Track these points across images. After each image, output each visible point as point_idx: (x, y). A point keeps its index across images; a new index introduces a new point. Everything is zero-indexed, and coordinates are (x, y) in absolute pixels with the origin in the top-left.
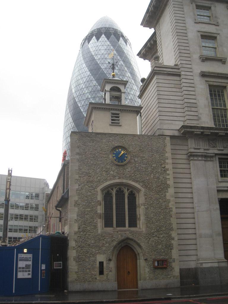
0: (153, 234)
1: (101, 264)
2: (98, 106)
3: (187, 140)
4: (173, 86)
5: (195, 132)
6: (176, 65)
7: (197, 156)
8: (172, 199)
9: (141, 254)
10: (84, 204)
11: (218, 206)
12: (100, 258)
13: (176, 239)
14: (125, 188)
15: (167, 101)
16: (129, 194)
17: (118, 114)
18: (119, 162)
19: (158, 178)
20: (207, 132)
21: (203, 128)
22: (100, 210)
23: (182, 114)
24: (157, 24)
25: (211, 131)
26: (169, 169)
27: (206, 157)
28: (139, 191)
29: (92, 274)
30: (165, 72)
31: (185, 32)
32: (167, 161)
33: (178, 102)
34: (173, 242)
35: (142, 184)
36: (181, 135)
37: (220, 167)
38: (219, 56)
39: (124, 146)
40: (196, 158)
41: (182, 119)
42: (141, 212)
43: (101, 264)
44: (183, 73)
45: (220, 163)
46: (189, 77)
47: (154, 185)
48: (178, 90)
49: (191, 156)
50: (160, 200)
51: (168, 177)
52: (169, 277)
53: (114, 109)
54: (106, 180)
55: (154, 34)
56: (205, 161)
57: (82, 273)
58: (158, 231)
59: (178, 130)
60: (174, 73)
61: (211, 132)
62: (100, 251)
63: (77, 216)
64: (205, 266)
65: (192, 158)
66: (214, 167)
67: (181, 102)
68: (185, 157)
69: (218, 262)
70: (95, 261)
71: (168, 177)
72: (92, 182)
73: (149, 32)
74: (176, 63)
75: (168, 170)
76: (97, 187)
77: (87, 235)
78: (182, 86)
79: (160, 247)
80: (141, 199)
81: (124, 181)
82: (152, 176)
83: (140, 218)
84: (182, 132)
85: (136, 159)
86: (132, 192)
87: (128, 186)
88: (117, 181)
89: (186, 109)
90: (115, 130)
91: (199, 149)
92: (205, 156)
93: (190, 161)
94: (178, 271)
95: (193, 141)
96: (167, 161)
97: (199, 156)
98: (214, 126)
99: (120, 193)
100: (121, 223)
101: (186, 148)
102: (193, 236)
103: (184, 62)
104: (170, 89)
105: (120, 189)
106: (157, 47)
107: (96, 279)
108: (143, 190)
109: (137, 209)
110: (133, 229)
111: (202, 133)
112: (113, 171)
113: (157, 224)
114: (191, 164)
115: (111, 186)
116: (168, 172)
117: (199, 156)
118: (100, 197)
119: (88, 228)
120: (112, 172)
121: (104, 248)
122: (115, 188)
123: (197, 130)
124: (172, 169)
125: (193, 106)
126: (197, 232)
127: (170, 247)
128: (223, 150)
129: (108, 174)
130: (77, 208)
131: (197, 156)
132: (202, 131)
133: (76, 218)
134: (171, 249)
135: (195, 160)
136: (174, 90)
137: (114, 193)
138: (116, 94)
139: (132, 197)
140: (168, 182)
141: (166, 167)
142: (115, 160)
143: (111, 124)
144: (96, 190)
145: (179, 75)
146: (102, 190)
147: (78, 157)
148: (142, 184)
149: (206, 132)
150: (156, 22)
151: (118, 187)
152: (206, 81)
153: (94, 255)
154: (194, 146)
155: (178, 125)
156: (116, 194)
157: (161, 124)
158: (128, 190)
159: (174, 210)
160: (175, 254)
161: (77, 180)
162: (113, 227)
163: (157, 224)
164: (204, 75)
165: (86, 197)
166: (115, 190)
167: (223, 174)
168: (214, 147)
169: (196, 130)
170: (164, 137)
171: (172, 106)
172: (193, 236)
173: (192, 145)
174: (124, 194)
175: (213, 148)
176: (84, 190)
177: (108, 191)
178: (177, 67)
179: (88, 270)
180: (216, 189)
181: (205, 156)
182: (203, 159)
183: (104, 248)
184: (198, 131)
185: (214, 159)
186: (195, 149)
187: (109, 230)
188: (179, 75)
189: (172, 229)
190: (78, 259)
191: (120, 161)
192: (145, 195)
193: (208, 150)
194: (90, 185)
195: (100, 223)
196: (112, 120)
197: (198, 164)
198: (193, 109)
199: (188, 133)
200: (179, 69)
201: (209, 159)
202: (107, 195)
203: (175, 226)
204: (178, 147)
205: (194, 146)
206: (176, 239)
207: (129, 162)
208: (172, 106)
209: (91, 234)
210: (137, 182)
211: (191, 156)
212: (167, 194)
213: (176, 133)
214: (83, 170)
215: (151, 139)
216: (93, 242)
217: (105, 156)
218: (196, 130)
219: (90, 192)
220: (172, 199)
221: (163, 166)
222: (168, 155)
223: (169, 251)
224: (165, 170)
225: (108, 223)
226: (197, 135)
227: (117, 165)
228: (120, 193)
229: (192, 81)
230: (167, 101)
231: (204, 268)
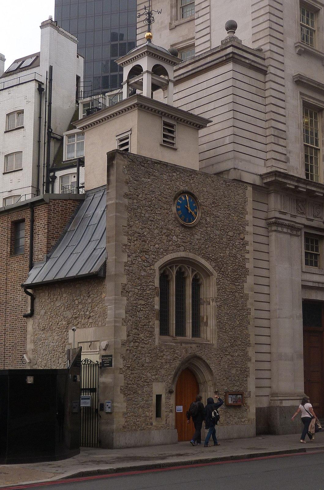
0: (226, 351)
1: (159, 397)
3: (268, 193)
4: (254, 90)
5: (288, 186)
6: (259, 50)
8: (251, 294)
9: (210, 383)
10: (136, 291)
11: (299, 312)
12: (159, 388)
14: (189, 268)
17: (172, 126)
18: (185, 220)
19: (235, 257)
20: (291, 184)
25: (308, 187)
26: (249, 243)
27: (293, 229)
28: (208, 274)
29: (146, 416)
30: (247, 61)
35: (214, 264)
36: (264, 185)
37: (307, 247)
38: (317, 49)
39: (192, 192)
40: (280, 229)
43: (159, 397)
45: (307, 240)
48: (260, 100)
49: (273, 224)
50: (237, 294)
51: (247, 256)
52: (243, 420)
54: (167, 251)
56: (291, 235)
57: (132, 415)
58: (232, 346)
59: (261, 175)
61: (307, 189)
62: (157, 376)
63: (126, 313)
65: (274, 228)
66: (297, 246)
70: (150, 394)
72: (146, 252)
75: (247, 244)
76: (154, 261)
77: (140, 348)
79: (234, 371)
81: (191, 255)
82: (228, 252)
83: (207, 322)
84: (265, 181)
85: (208, 219)
88: (182, 254)
89: (272, 139)
90: (167, 157)
91: (284, 213)
93: (269, 232)
94: (254, 411)
98: (305, 178)
101: (264, 207)
104: (250, 96)
107: (152, 424)
108: (215, 273)
109: (202, 307)
112: (177, 236)
113: (231, 333)
116: (247, 248)
117: (285, 225)
119: (141, 335)
120: (175, 238)
122: (176, 266)
123: (292, 183)
124: (252, 243)
125: (280, 136)
127: (245, 372)
128: (312, 220)
129: (170, 241)
130: (125, 298)
131: (282, 225)
132: (296, 184)
133: (124, 317)
135: (279, 232)
140: (247, 265)
141: (246, 239)
142: (180, 217)
144: (152, 267)
145: (264, 73)
146: (160, 268)
147: (126, 201)
148: (214, 264)
151: (180, 265)
153: (149, 383)
154: (279, 207)
158: (193, 271)
159: (253, 313)
160: (251, 386)
161: (126, 245)
164: (299, 81)
165: (138, 278)
167: (311, 259)
168: (302, 213)
169: (289, 182)
170: (245, 185)
173: (275, 205)
175: (301, 216)
176: (135, 266)
179: (140, 410)
180: (300, 283)
186: (281, 212)
188: (265, 73)
189: (248, 344)
191: (186, 217)
192: (218, 284)
193: (295, 216)
194: (143, 258)
198: (281, 142)
199: (276, 184)
200: (264, 59)
202: (164, 278)
203: (252, 339)
205: (279, 207)
206: (253, 360)
207: (199, 223)
209: (146, 346)
210: (208, 259)
211: (275, 224)
212: (245, 284)
213: (258, 181)
214: (134, 228)
216: (148, 360)
217: (165, 206)
218: (289, 182)
219: (145, 270)
220: (251, 294)
221: (242, 236)
223: (245, 379)
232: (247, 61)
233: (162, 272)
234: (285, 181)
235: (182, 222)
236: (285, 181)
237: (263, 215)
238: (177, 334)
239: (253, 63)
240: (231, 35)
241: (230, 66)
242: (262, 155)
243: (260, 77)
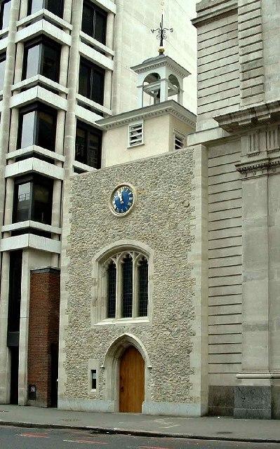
2: (131, 117)
7: (250, 169)
12: (93, 364)
18: (120, 212)
21: (252, 110)
22: (100, 291)
25: (271, 111)
32: (193, 193)
34: (193, 339)
40: (250, 175)
47: (170, 242)
51: (192, 222)
53: (133, 120)
64: (245, 383)
69: (272, 378)
71: (192, 222)
75: (193, 210)
81: (125, 242)
87: (136, 250)
96: (193, 193)
99: (127, 263)
100: (126, 313)
105: (128, 255)
111: (254, 120)
115: (113, 253)
121: (97, 349)
123: (243, 118)
131: (250, 169)
132: (251, 116)
134: (189, 352)
137: (117, 262)
143: (130, 146)
146: (101, 261)
149: (261, 116)
158: (137, 254)
163: (169, 308)
169: (239, 119)
173: (245, 151)
182: (265, 172)
183: (97, 349)
186: (250, 156)
187: (109, 321)
190: (69, 368)
202: (111, 270)
210: (144, 239)
213: (217, 134)
215: (171, 158)
218: (239, 119)
224: (188, 209)
225: (111, 314)
226: (245, 127)
227: (118, 218)
228: (127, 263)
231: (243, 387)
233: (108, 262)
234: (233, 121)
235: (125, 214)
236: (233, 121)
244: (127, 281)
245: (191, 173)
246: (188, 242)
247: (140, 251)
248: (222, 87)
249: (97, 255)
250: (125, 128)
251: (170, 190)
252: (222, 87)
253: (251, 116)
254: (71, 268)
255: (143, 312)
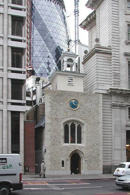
7: (116, 106)
13: (102, 150)
15: (102, 71)
16: (78, 126)
20: (124, 92)
21: (122, 90)
22: (62, 134)
23: (110, 69)
24: (97, 8)
27: (121, 107)
28: (83, 124)
30: (102, 52)
31: (117, 21)
32: (99, 108)
33: (108, 72)
40: (116, 107)
41: (110, 83)
42: (84, 136)
44: (113, 53)
46: (117, 56)
49: (114, 106)
51: (100, 117)
55: (95, 12)
59: (107, 90)
60: (106, 52)
67: (110, 72)
68: (110, 106)
73: (90, 11)
74: (109, 45)
78: (112, 61)
80: (84, 129)
86: (79, 125)
87: (78, 122)
91: (118, 102)
92: (121, 106)
95: (115, 97)
97: (118, 106)
99: (73, 126)
100: (73, 142)
101: (110, 100)
102: (111, 149)
103: (115, 45)
104: (105, 63)
105: (73, 123)
106: (96, 21)
109: (82, 134)
110: (79, 145)
114: (113, 110)
115: (69, 121)
117: (118, 106)
118: (62, 127)
125: (116, 76)
126: (113, 148)
131: (116, 106)
132: (121, 92)
134: (99, 155)
136: (106, 64)
137: (70, 125)
138: (70, 63)
139: (79, 128)
145: (111, 54)
146: (64, 124)
150: (97, 6)
152: (127, 59)
155: (108, 87)
156: (71, 126)
157: (97, 85)
158: (77, 124)
162: (69, 143)
166: (70, 123)
171: (105, 74)
172: (111, 149)
173: (114, 100)
174: (75, 126)
177: (67, 124)
178: (109, 48)
180: (125, 125)
181: (121, 106)
184: (119, 92)
185: (126, 108)
188: (111, 54)
193: (123, 103)
195: (62, 140)
196: (69, 81)
197: (117, 111)
199: (112, 93)
201: (123, 108)
202: (66, 127)
204: (106, 100)
208: (105, 74)
213: (105, 92)
222: (101, 105)
224: (98, 113)
225: (66, 141)
228: (73, 126)
229: (118, 59)
230: (102, 71)
232: (102, 52)
233: (65, 124)
234: (116, 91)
237: (110, 103)
238: (71, 143)
239: (105, 52)
240: (97, 43)
241: (96, 54)
242: (110, 83)
243: (109, 56)
244: (72, 132)
245: (99, 102)
246: (98, 123)
247: (79, 122)
248: (105, 77)
249: (64, 121)
250: (66, 77)
251: (92, 105)
252: (105, 77)
253: (121, 92)
254: (51, 124)
255: (79, 141)
